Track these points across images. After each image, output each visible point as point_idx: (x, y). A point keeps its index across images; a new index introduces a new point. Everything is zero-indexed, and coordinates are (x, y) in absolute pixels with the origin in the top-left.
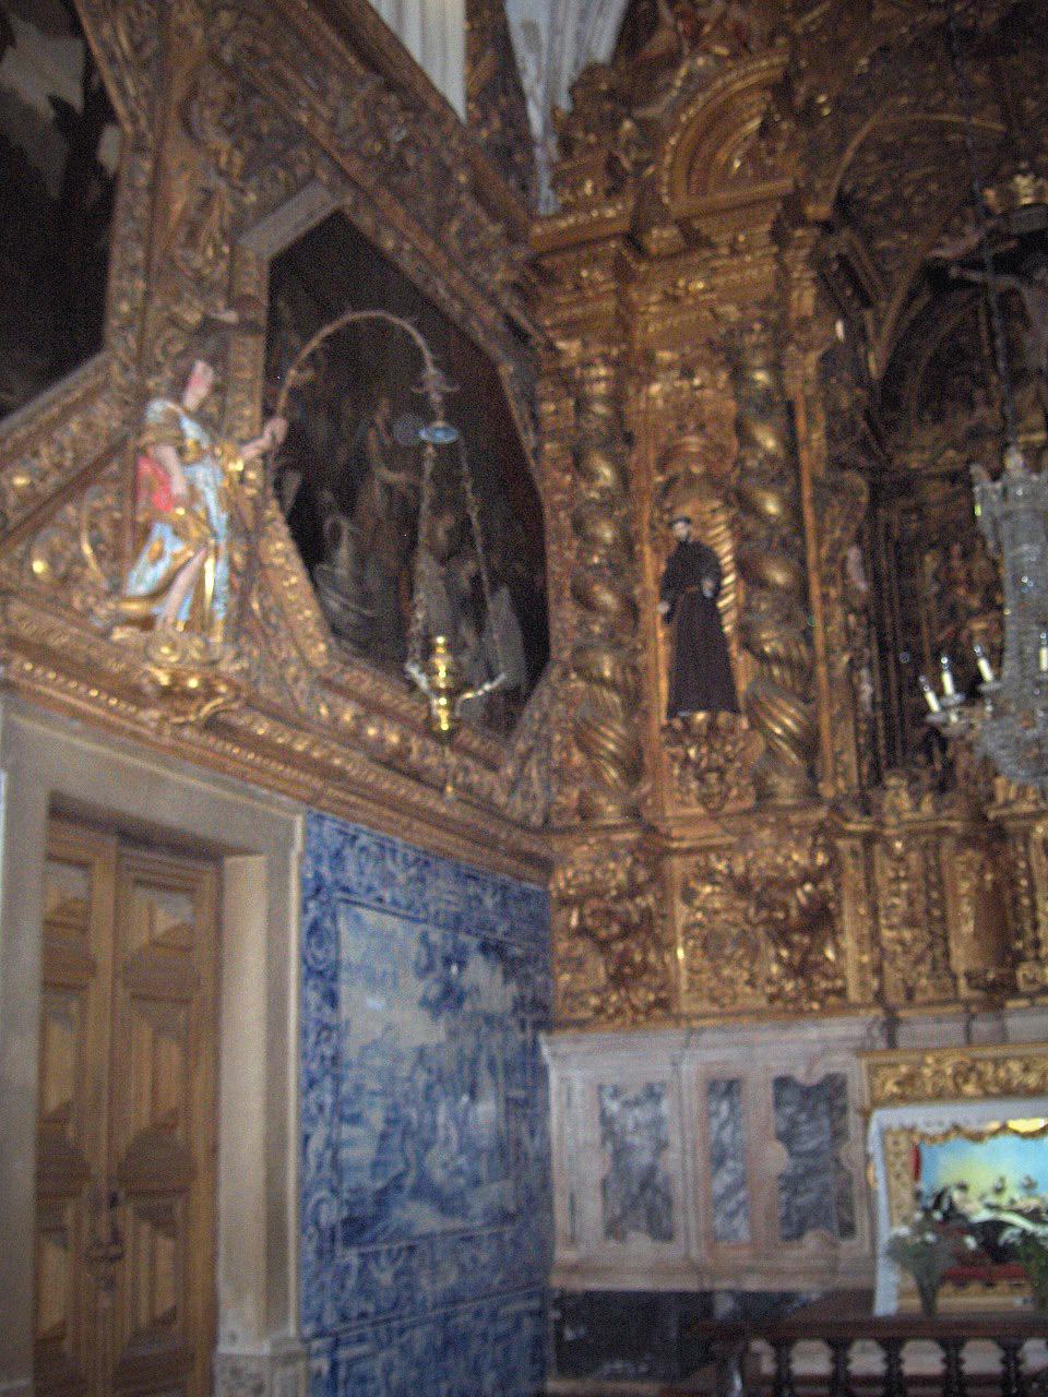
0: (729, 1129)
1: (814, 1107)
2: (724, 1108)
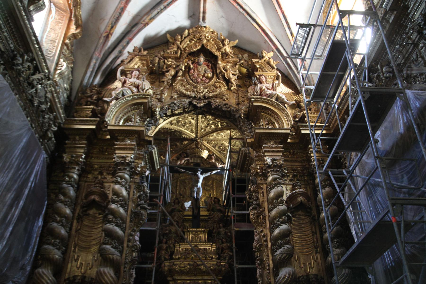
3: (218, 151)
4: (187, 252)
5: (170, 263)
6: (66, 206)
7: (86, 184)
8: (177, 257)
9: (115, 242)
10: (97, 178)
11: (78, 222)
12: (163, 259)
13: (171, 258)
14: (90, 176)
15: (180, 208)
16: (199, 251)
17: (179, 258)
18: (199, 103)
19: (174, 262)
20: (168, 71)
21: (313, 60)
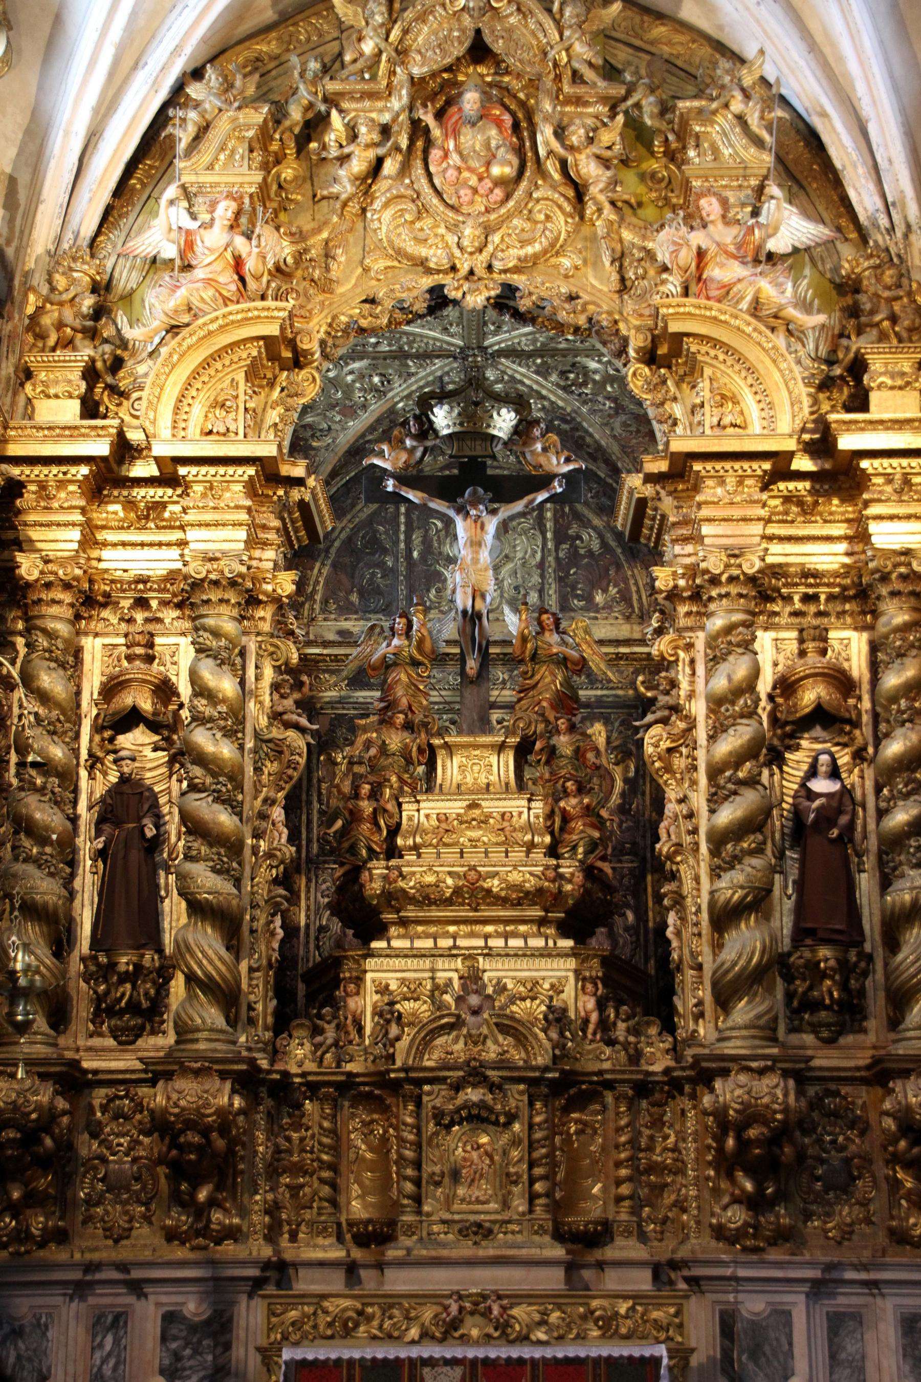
0: (112, 1362)
1: (199, 1342)
2: (109, 1340)
3: (558, 385)
4: (444, 826)
5: (387, 868)
6: (55, 738)
7: (99, 641)
8: (410, 842)
9: (219, 854)
10: (131, 621)
11: (91, 777)
12: (364, 852)
13: (392, 852)
14: (105, 614)
15: (415, 653)
16: (485, 822)
17: (416, 848)
18: (471, 291)
19: (398, 868)
20: (344, 159)
21: (880, 205)
